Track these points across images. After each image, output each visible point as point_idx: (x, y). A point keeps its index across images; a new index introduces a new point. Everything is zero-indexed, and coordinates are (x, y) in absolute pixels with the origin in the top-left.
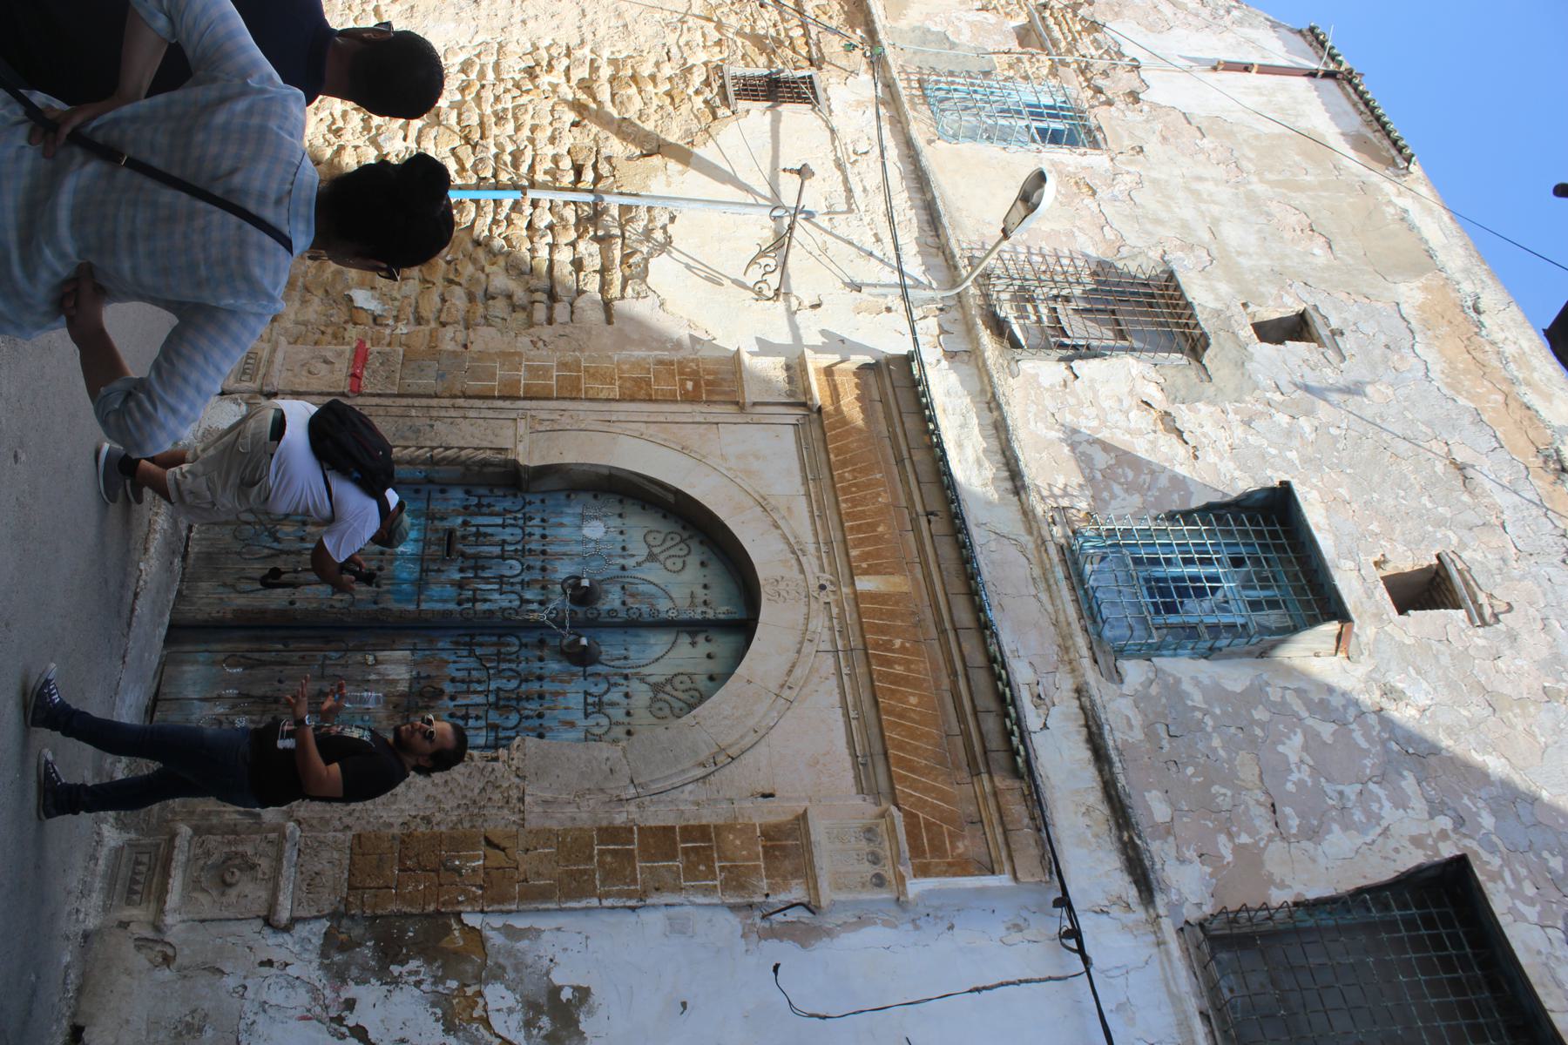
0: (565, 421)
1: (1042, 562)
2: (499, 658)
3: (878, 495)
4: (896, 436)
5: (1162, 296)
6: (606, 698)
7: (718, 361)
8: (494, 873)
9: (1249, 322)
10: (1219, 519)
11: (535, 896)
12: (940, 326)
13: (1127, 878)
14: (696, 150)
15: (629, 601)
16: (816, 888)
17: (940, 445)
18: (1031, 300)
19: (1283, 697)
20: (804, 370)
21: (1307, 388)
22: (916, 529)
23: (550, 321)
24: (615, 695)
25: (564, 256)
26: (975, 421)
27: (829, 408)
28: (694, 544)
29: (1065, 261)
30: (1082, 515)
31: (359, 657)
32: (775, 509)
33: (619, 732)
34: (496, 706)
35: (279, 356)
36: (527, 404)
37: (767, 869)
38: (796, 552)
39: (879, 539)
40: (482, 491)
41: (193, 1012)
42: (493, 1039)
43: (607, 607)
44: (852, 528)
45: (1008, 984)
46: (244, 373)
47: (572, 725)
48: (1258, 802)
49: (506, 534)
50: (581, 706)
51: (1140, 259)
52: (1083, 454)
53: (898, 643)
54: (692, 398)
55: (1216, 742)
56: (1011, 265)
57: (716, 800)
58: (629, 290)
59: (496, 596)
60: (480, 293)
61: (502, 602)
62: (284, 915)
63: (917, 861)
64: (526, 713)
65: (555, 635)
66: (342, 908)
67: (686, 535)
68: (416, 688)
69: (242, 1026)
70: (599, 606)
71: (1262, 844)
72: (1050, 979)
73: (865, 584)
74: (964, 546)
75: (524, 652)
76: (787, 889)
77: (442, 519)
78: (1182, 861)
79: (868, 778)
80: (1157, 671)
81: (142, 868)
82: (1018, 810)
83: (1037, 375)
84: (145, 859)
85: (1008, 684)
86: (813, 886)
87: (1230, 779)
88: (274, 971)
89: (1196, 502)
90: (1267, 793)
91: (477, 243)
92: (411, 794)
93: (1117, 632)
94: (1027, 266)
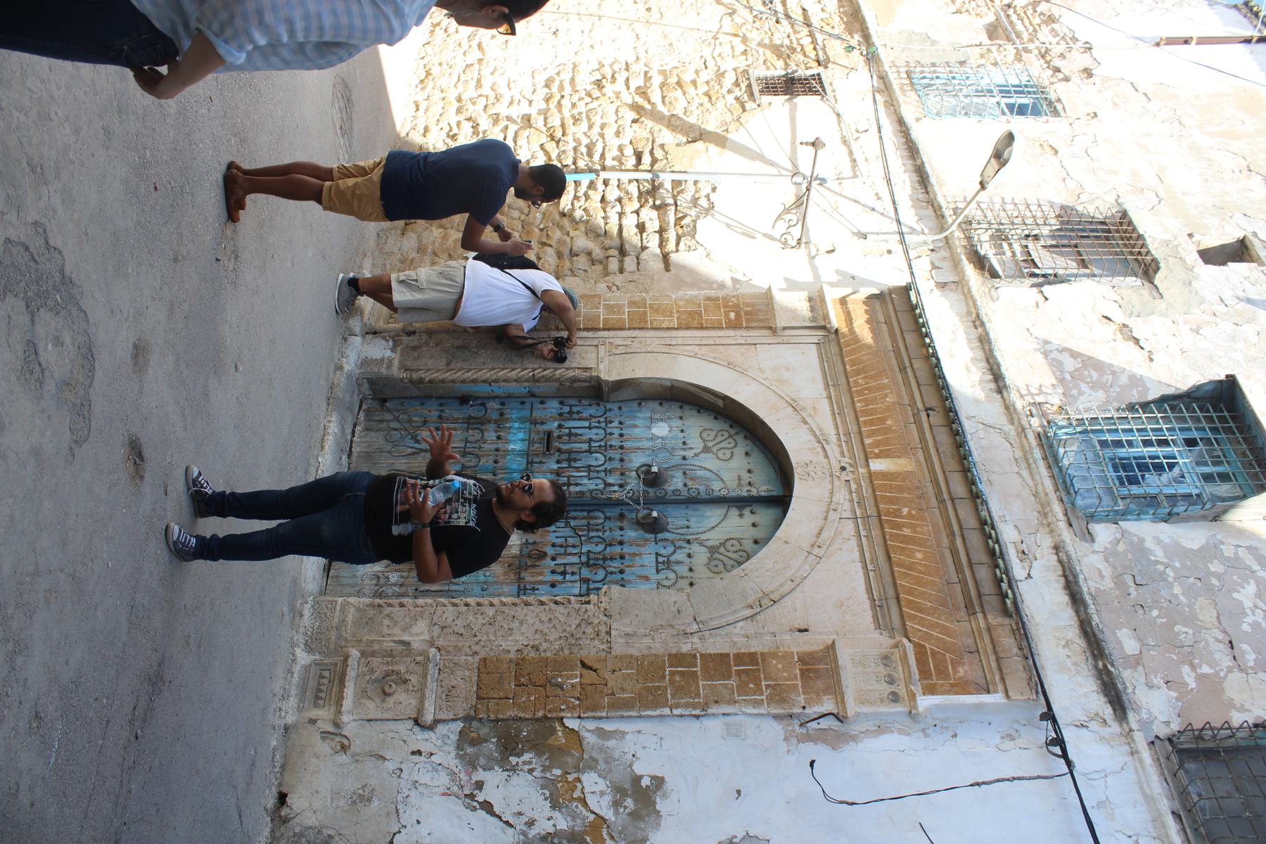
0: (636, 346)
1: (1022, 446)
2: (589, 528)
3: (886, 396)
5: (1118, 231)
6: (673, 558)
7: (755, 296)
8: (589, 688)
9: (1194, 249)
10: (1173, 408)
11: (620, 706)
13: (1103, 699)
14: (729, 136)
15: (689, 483)
16: (843, 701)
17: (935, 355)
18: (1007, 239)
20: (823, 300)
21: (1249, 301)
22: (918, 422)
23: (621, 271)
24: (680, 556)
25: (630, 222)
27: (844, 329)
28: (740, 439)
29: (1033, 208)
30: (1055, 408)
32: (804, 409)
33: (684, 583)
34: (587, 564)
36: (606, 334)
38: (821, 442)
39: (888, 430)
41: (364, 786)
42: (589, 814)
43: (672, 488)
44: (865, 422)
45: (1003, 780)
47: (647, 578)
48: (1217, 640)
49: (592, 434)
50: (654, 564)
51: (1097, 203)
53: (905, 511)
54: (734, 326)
55: (1177, 590)
56: (989, 214)
57: (762, 634)
58: (682, 244)
59: (585, 481)
60: (566, 252)
61: (589, 485)
62: (429, 717)
64: (610, 569)
65: (632, 511)
66: (472, 713)
67: (733, 432)
68: (525, 551)
69: (400, 798)
70: (666, 487)
71: (1222, 674)
72: (1039, 777)
73: (877, 465)
74: (958, 434)
75: (608, 524)
76: (819, 702)
77: (542, 423)
79: (884, 617)
81: (325, 681)
82: (1008, 642)
84: (326, 674)
85: (997, 541)
86: (841, 700)
87: (1191, 620)
88: (422, 758)
89: (1153, 395)
90: (1224, 632)
91: (563, 215)
92: (523, 629)
93: (1088, 501)
94: (1002, 214)
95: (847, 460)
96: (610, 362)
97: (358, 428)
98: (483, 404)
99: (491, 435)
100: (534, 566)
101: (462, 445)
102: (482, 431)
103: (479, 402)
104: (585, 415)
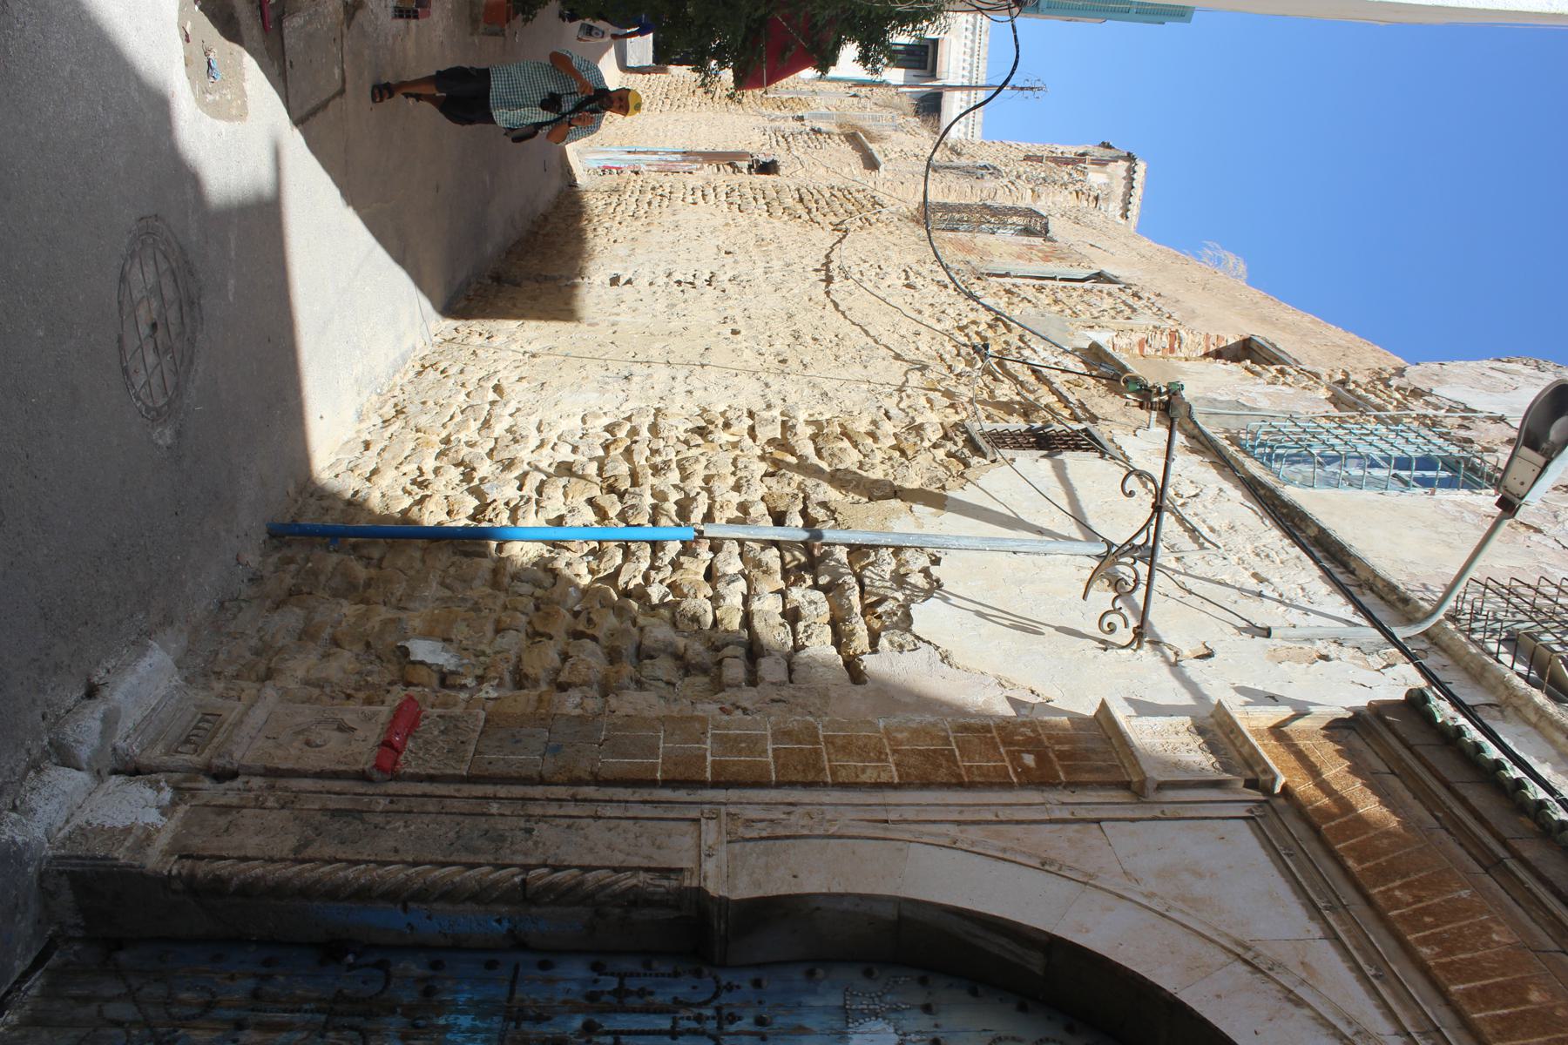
14: (949, 493)
25: (768, 605)
36: (720, 795)
40: (626, 965)
46: (187, 741)
54: (1041, 780)
77: (539, 1019)
98: (382, 965)
104: (659, 999)
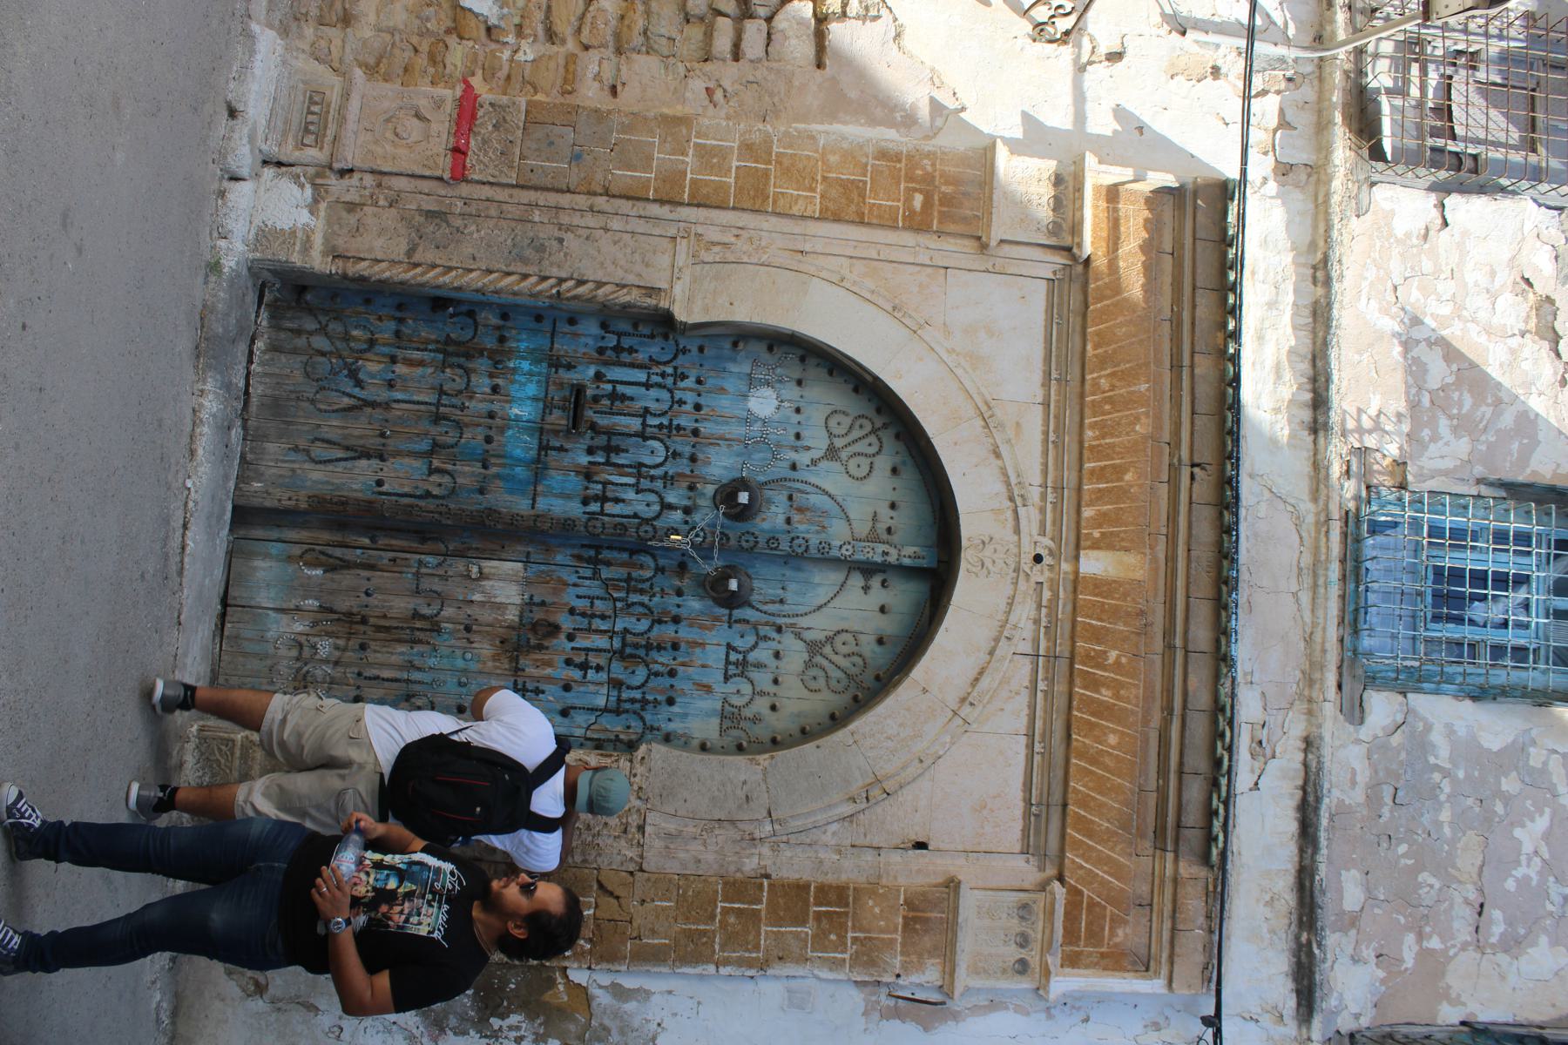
1: (1317, 548)
2: (630, 584)
3: (1137, 419)
4: (1180, 324)
6: (752, 657)
11: (649, 957)
12: (1282, 112)
13: (1290, 985)
15: (796, 517)
17: (1235, 359)
19: (1545, 763)
20: (1079, 190)
22: (1174, 484)
23: (736, 55)
24: (763, 654)
26: (1290, 298)
27: (1100, 262)
28: (887, 436)
31: (459, 565)
32: (1001, 426)
34: (620, 654)
35: (355, 104)
37: (903, 945)
39: (1121, 494)
44: (1092, 471)
46: (307, 131)
47: (708, 689)
49: (652, 399)
50: (722, 665)
52: (1416, 360)
54: (918, 224)
55: (1445, 816)
59: (630, 495)
61: (639, 504)
63: (1067, 949)
64: (656, 667)
71: (1451, 953)
73: (1094, 564)
75: (659, 579)
76: (920, 967)
77: (569, 367)
78: (1356, 959)
80: (1409, 712)
82: (1194, 905)
83: (1392, 213)
85: (1231, 723)
90: (1481, 891)
95: (1047, 541)
96: (694, 280)
97: (260, 344)
98: (471, 314)
99: (482, 383)
100: (540, 647)
101: (431, 398)
102: (468, 372)
103: (464, 308)
104: (641, 357)
